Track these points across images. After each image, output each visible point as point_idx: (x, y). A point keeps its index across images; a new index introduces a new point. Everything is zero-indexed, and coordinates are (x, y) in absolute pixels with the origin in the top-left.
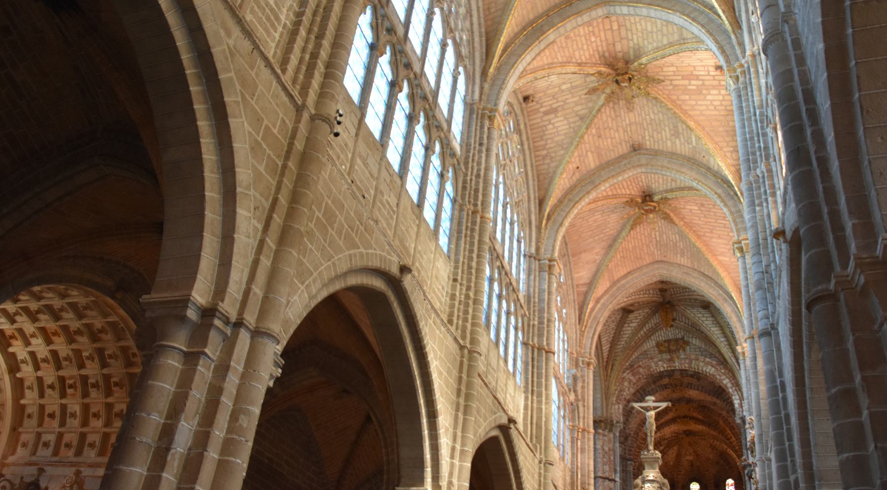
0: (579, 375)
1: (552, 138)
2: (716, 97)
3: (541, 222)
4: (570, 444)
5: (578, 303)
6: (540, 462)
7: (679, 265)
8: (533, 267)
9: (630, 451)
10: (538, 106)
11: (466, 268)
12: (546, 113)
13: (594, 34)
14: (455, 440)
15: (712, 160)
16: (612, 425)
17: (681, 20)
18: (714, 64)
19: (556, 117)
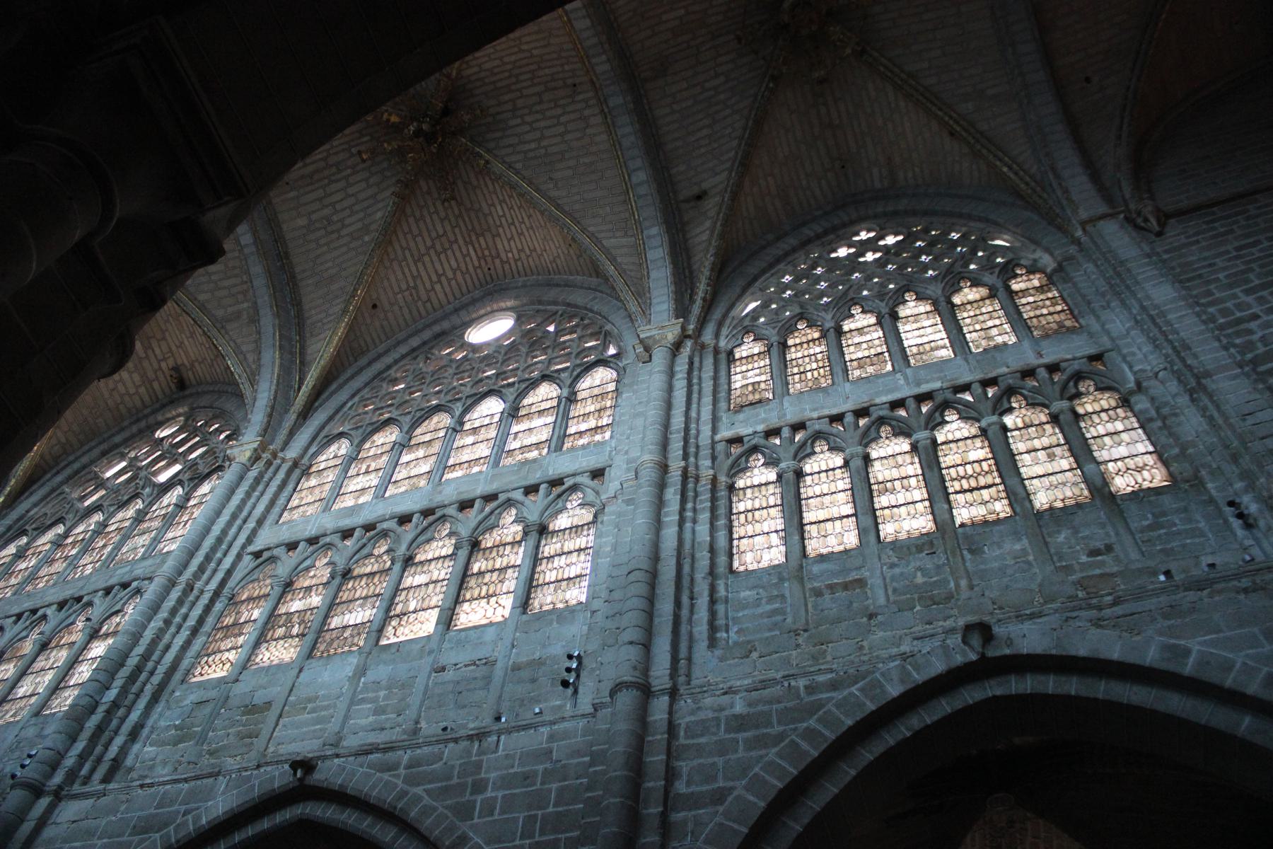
17: (271, 329)
18: (179, 362)
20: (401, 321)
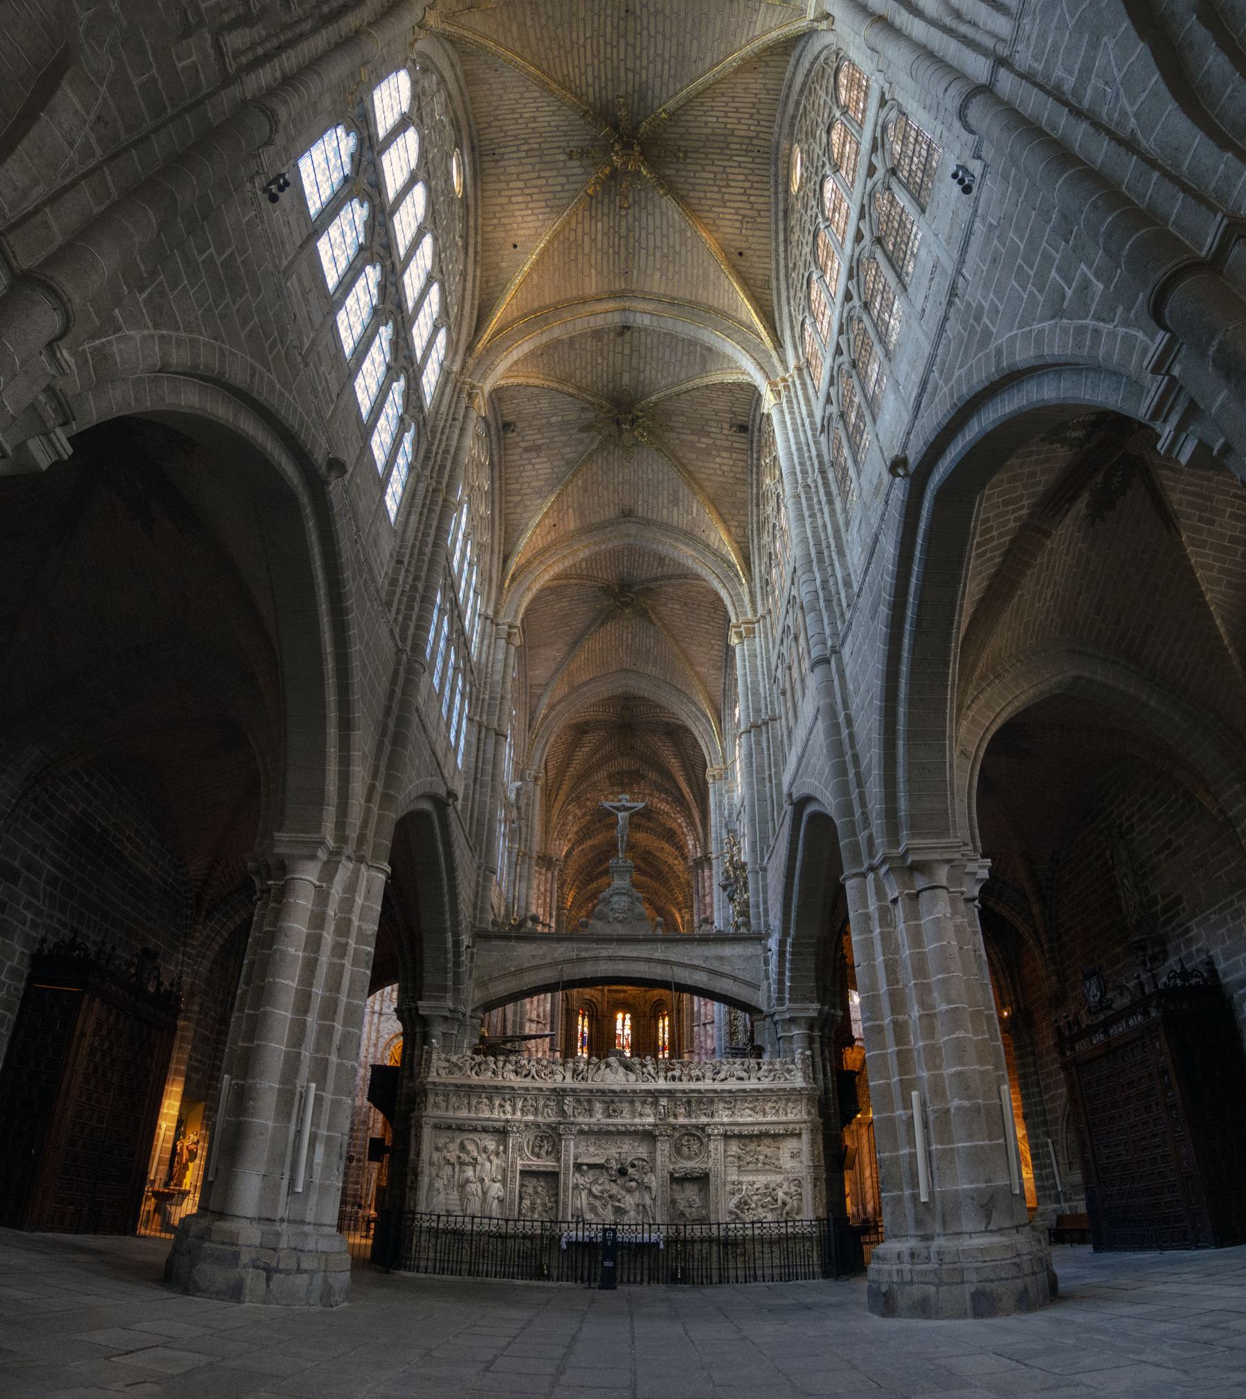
1: (529, 483)
2: (726, 461)
3: (503, 582)
6: (479, 868)
8: (488, 630)
10: (519, 439)
11: (416, 550)
12: (527, 450)
13: (602, 354)
14: (375, 776)
15: (713, 535)
19: (538, 456)
20: (763, 240)
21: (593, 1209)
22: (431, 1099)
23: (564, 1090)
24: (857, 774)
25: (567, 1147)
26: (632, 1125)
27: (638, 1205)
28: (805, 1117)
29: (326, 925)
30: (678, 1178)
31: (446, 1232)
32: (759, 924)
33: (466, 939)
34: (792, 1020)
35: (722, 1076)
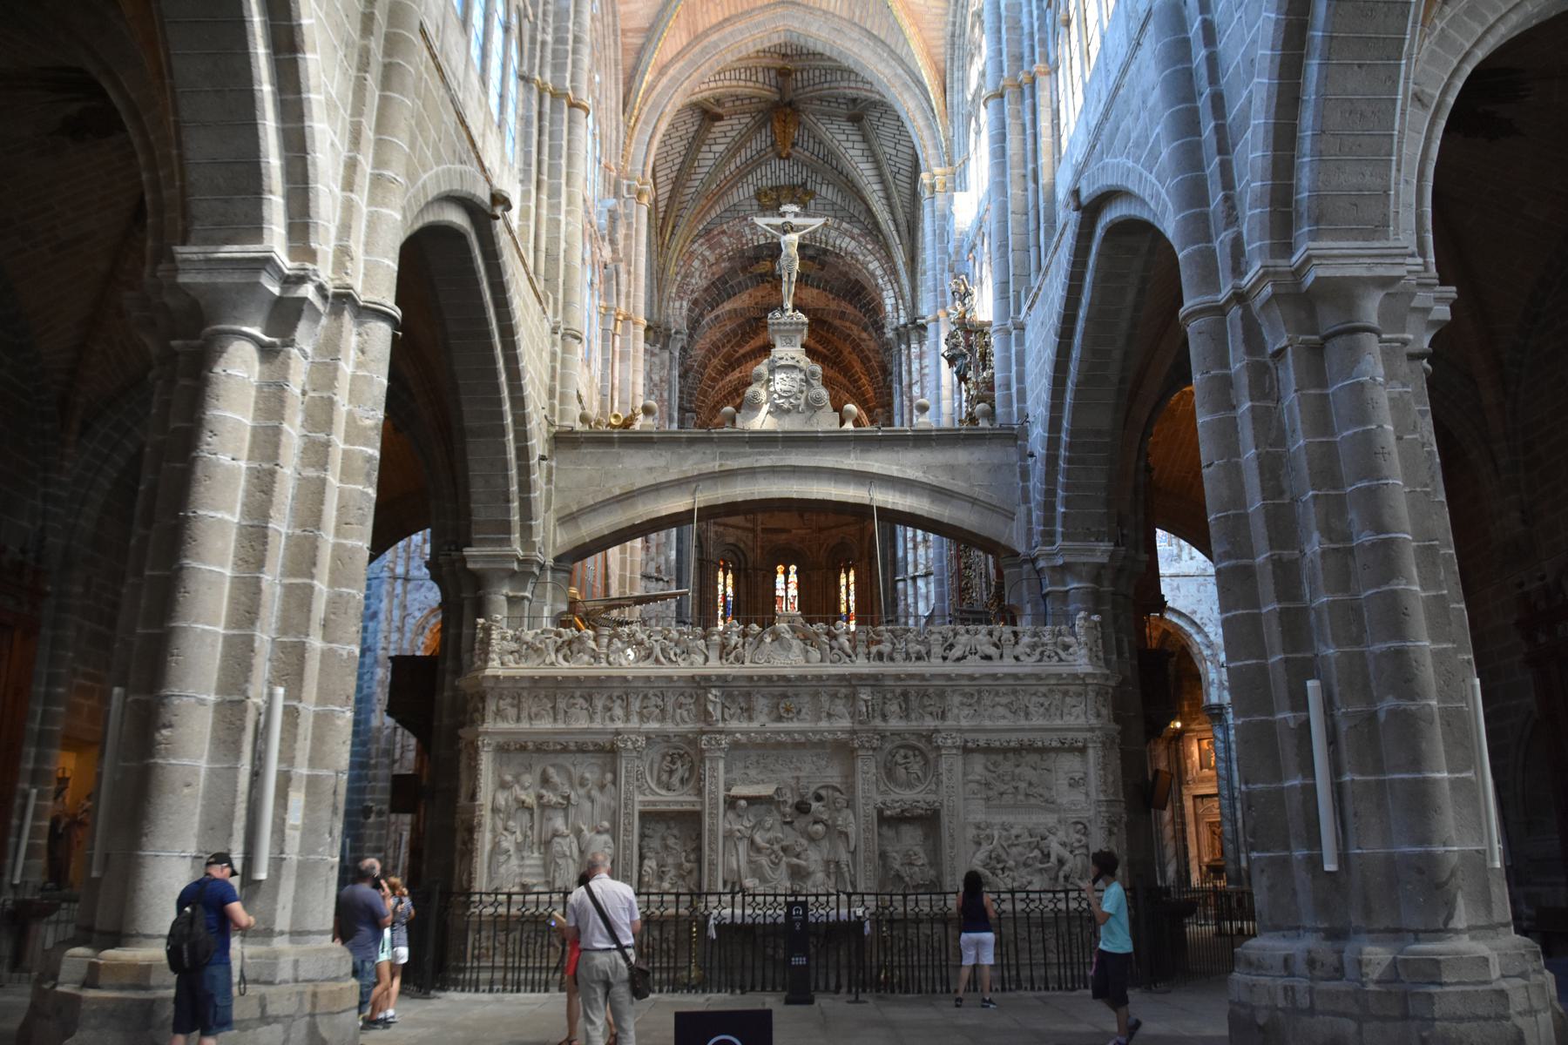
0: (621, 210)
4: (599, 342)
5: (624, 69)
6: (554, 331)
7: (825, 12)
9: (691, 395)
16: (669, 336)
21: (756, 871)
22: (491, 706)
23: (707, 678)
24: (1220, 130)
25: (713, 769)
26: (814, 732)
27: (827, 863)
28: (1093, 721)
29: (288, 413)
30: (891, 817)
31: (522, 920)
32: (1010, 414)
33: (538, 444)
34: (1066, 568)
35: (957, 652)
